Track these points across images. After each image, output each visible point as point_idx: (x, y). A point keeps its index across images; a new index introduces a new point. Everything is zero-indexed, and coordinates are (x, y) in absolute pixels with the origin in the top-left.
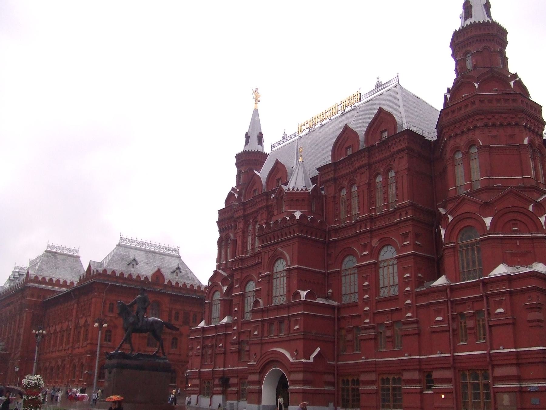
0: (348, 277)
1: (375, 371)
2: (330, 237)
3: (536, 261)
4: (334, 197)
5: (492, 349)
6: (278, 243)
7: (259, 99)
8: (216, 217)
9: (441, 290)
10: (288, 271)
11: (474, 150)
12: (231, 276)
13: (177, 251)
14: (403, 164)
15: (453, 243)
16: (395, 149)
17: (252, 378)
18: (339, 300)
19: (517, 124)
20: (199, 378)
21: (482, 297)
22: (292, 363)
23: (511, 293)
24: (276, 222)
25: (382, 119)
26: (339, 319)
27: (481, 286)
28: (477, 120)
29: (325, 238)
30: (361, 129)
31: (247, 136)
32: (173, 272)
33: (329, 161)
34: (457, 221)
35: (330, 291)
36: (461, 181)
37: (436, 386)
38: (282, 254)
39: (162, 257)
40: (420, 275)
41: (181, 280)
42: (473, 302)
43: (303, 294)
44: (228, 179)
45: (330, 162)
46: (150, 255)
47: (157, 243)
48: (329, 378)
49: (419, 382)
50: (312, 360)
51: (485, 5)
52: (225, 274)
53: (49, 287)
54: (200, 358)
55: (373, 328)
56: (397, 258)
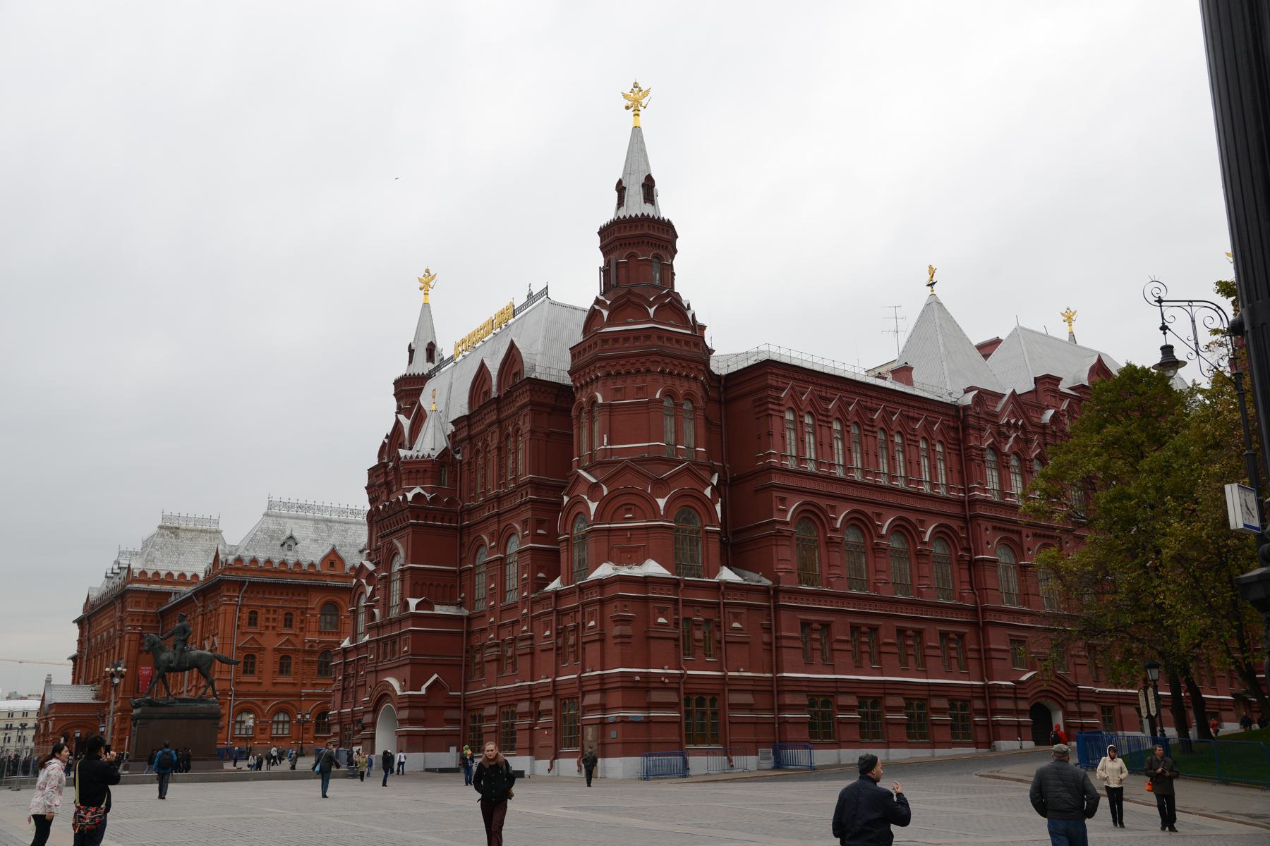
2: (463, 521)
4: (469, 463)
8: (365, 481)
19: (648, 371)
21: (577, 607)
23: (602, 602)
30: (494, 368)
31: (411, 351)
34: (572, 504)
37: (543, 720)
39: (343, 527)
40: (541, 575)
43: (413, 602)
46: (323, 526)
47: (335, 505)
48: (455, 714)
49: (530, 714)
50: (423, 692)
53: (167, 588)
56: (519, 552)
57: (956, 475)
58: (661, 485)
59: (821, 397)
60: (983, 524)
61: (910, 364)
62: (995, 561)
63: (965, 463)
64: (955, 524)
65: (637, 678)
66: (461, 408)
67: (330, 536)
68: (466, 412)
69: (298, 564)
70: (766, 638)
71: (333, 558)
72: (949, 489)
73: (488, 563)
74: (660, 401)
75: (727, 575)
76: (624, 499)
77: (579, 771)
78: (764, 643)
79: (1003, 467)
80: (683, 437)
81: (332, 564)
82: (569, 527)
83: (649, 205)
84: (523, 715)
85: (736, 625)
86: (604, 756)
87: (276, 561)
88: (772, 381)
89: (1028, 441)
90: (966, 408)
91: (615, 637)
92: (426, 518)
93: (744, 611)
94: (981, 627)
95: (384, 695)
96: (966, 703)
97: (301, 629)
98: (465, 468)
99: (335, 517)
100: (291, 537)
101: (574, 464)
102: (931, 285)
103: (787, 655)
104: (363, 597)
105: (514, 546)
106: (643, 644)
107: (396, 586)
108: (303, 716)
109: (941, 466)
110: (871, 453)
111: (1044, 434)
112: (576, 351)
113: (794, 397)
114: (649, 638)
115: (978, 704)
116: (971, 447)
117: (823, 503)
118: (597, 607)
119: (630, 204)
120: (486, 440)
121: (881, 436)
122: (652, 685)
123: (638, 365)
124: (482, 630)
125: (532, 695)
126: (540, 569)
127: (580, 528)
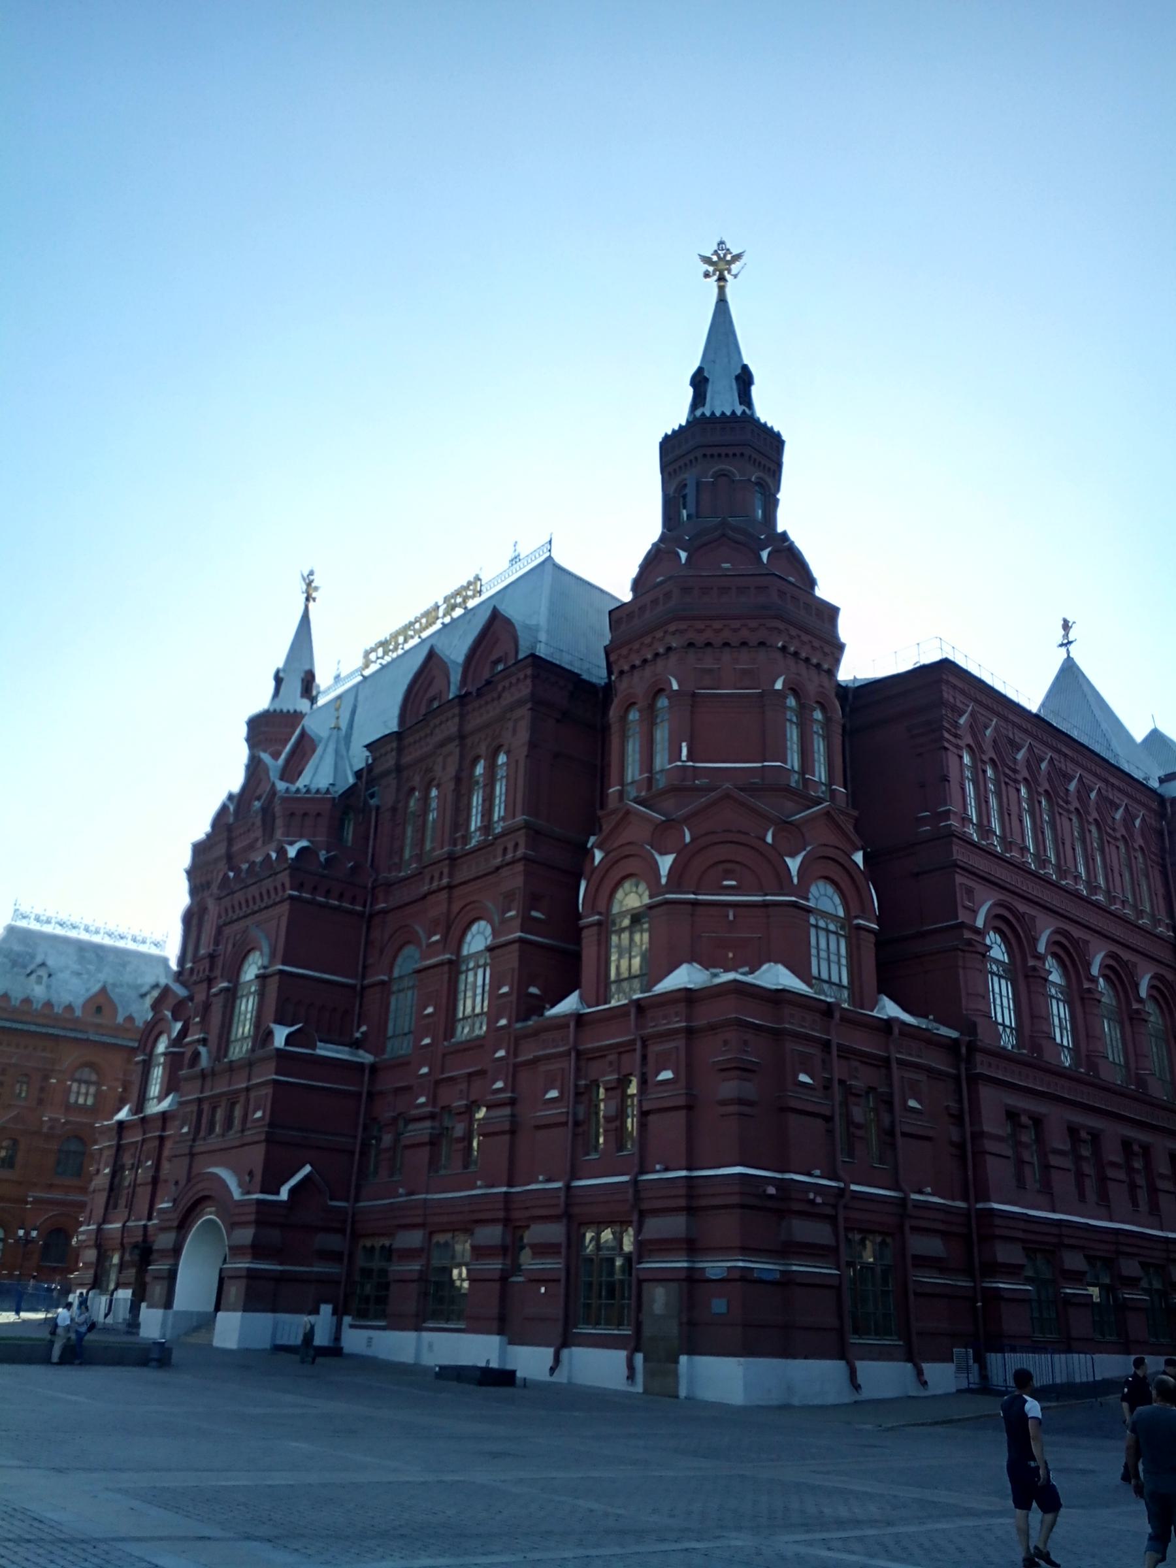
0: (402, 995)
1: (422, 1225)
3: (769, 961)
4: (394, 809)
5: (643, 1172)
7: (314, 595)
8: (186, 860)
9: (561, 1023)
11: (663, 702)
15: (600, 914)
18: (378, 1050)
22: (240, 1204)
27: (633, 1016)
28: (674, 633)
29: (364, 906)
31: (278, 680)
34: (610, 863)
35: (364, 1028)
36: (633, 772)
40: (533, 990)
42: (620, 1053)
43: (280, 1035)
45: (396, 729)
48: (334, 1242)
50: (284, 1195)
51: (738, 378)
55: (432, 1116)
65: (771, 1190)
67: (99, 970)
68: (393, 726)
69: (49, 1004)
70: (954, 1134)
72: (1157, 922)
73: (419, 971)
75: (890, 1009)
77: (631, 1377)
78: (952, 1143)
81: (99, 1009)
82: (601, 905)
85: (912, 1103)
86: (692, 1351)
88: (948, 695)
91: (723, 1103)
93: (922, 1077)
100: (43, 964)
105: (478, 939)
107: (247, 1007)
108: (27, 1233)
118: (681, 1043)
120: (429, 770)
122: (796, 1206)
123: (745, 634)
124: (398, 1091)
127: (631, 898)
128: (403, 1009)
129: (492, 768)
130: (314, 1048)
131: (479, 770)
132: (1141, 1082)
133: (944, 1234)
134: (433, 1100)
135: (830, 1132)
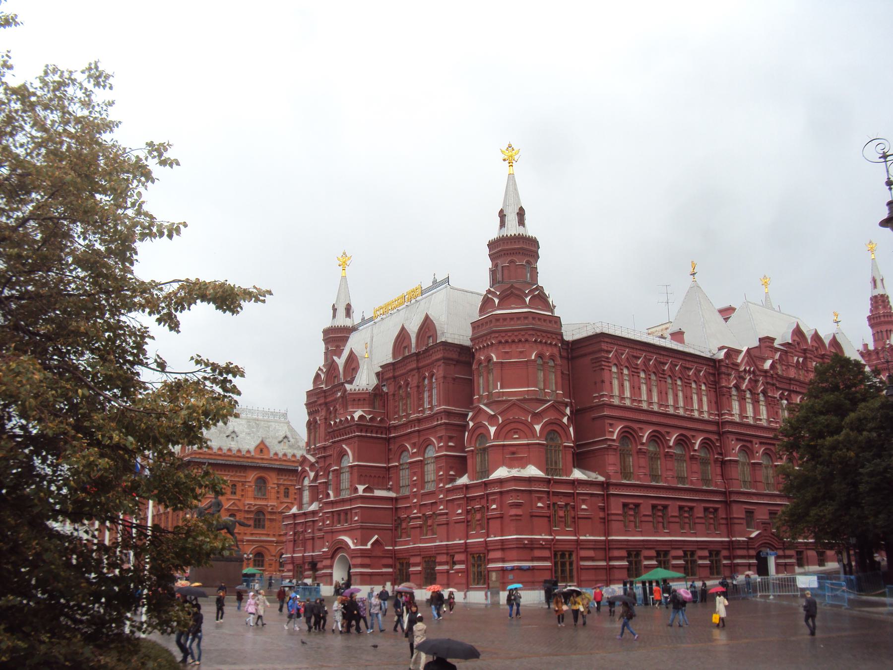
2: (390, 433)
4: (394, 395)
6: (343, 440)
8: (304, 399)
10: (351, 467)
12: (317, 462)
13: (285, 415)
14: (439, 371)
16: (434, 358)
17: (327, 562)
20: (293, 563)
23: (501, 493)
24: (341, 421)
25: (427, 326)
26: (397, 509)
31: (335, 310)
32: (280, 442)
33: (389, 359)
38: (346, 451)
40: (452, 473)
41: (290, 451)
43: (361, 488)
44: (314, 357)
48: (390, 561)
49: (446, 563)
50: (369, 546)
52: (313, 460)
54: (292, 543)
57: (713, 404)
58: (537, 416)
59: (634, 356)
60: (731, 437)
61: (683, 330)
62: (736, 461)
63: (719, 396)
64: (714, 437)
66: (386, 357)
69: (239, 451)
70: (602, 515)
71: (262, 446)
72: (710, 414)
74: (534, 361)
75: (577, 474)
76: (513, 426)
77: (487, 598)
78: (601, 518)
79: (742, 399)
80: (549, 386)
81: (261, 451)
83: (521, 227)
84: (441, 564)
85: (584, 507)
87: (225, 449)
88: (604, 346)
89: (757, 381)
90: (720, 361)
92: (366, 432)
94: (727, 504)
95: (339, 548)
96: (718, 553)
97: (242, 495)
98: (391, 398)
99: (261, 418)
100: (234, 432)
101: (475, 401)
102: (693, 274)
103: (615, 525)
104: (307, 479)
105: (431, 453)
106: (530, 520)
109: (705, 399)
110: (664, 392)
111: (766, 377)
112: (475, 326)
113: (618, 356)
114: (532, 516)
115: (725, 553)
116: (723, 387)
117: (636, 426)
119: (510, 226)
121: (669, 381)
123: (520, 337)
125: (449, 551)
126: (451, 468)
128: (405, 476)
129: (431, 383)
130: (373, 492)
131: (426, 382)
132: (692, 483)
133: (593, 549)
134: (419, 512)
135: (549, 521)
